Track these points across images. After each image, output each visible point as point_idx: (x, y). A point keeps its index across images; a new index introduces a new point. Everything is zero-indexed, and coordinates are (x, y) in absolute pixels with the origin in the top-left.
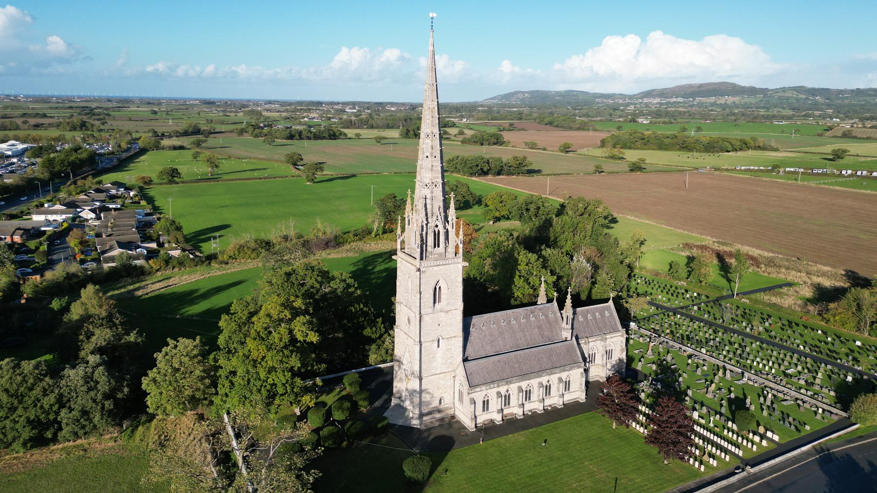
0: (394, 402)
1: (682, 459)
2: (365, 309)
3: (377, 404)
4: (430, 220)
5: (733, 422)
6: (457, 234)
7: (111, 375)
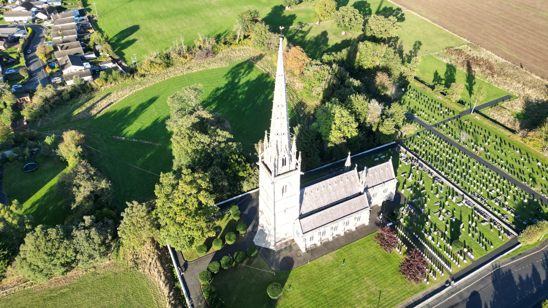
0: (259, 228)
1: (417, 280)
2: (239, 160)
3: (250, 228)
4: (280, 153)
5: (451, 245)
6: (297, 158)
7: (100, 234)
